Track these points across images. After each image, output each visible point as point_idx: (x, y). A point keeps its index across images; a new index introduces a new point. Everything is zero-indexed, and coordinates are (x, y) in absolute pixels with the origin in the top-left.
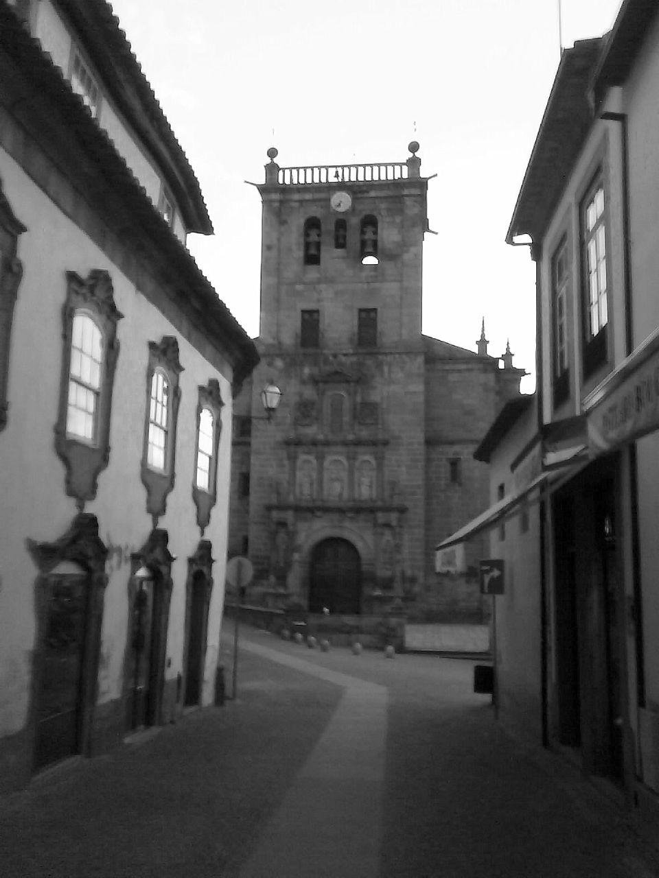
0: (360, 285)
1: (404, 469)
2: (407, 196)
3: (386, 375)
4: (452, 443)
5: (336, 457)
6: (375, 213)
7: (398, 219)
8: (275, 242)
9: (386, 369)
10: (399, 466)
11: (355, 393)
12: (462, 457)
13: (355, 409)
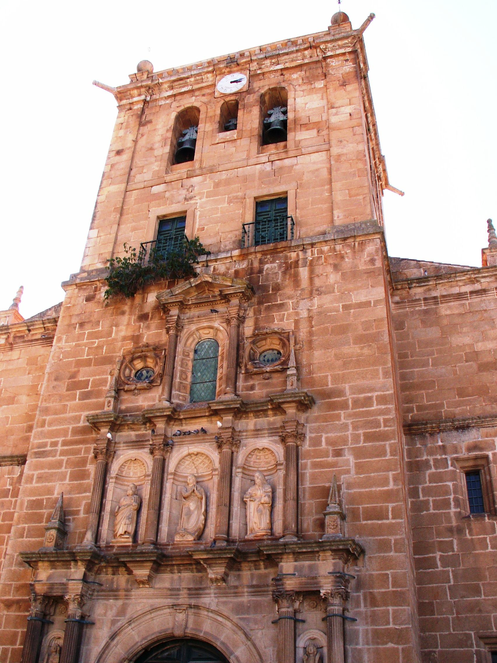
0: (258, 167)
1: (349, 458)
2: (331, 57)
3: (304, 282)
4: (464, 428)
5: (194, 449)
6: (283, 85)
7: (320, 84)
8: (129, 144)
9: (304, 272)
10: (338, 453)
11: (241, 320)
12: (490, 454)
13: (239, 347)
